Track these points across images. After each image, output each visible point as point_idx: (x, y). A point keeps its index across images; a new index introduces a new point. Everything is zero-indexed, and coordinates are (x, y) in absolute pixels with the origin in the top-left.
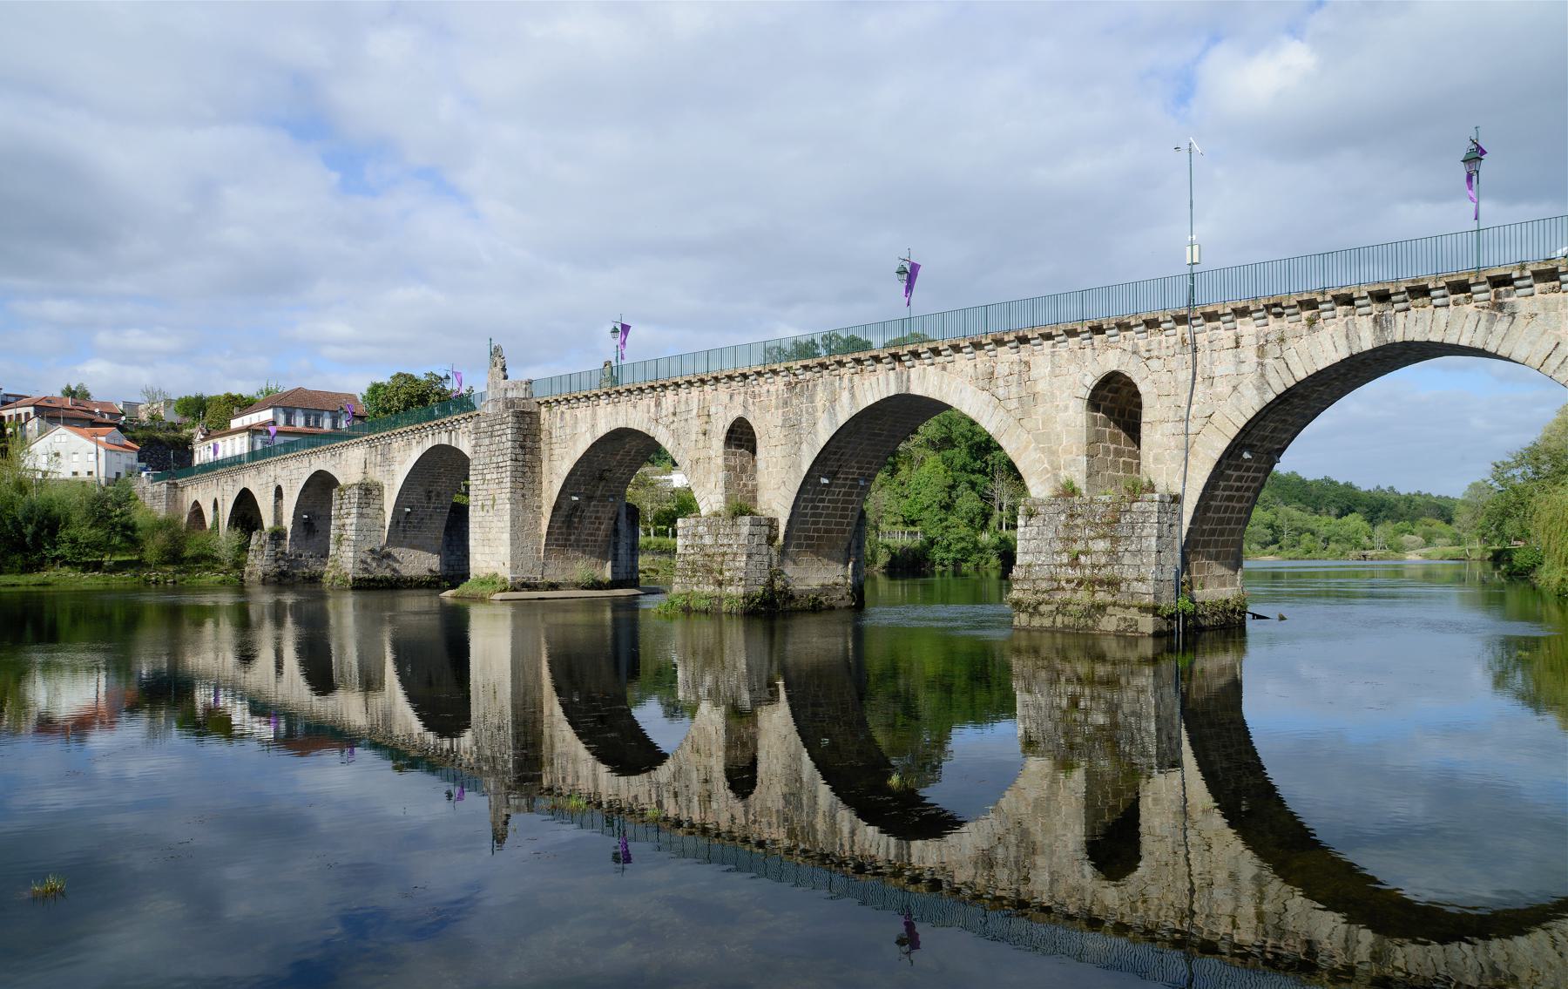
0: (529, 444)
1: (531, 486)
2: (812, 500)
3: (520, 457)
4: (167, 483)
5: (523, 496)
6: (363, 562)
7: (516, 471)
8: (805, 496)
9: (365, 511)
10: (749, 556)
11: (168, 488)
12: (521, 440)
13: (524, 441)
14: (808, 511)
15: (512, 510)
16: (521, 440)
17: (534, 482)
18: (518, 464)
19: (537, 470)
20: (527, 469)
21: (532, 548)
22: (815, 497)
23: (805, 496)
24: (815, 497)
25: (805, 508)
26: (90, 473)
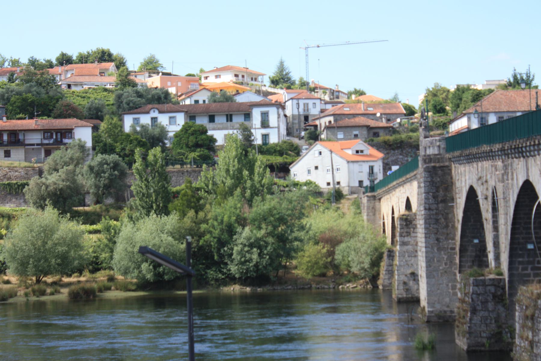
0: (441, 193)
1: (445, 231)
2: (529, 263)
3: (434, 207)
4: (367, 196)
5: (438, 239)
6: (405, 283)
7: (430, 218)
8: (520, 259)
9: (406, 239)
10: (474, 311)
11: (368, 200)
12: (434, 191)
13: (437, 191)
14: (529, 271)
15: (426, 252)
16: (434, 191)
17: (447, 226)
18: (432, 212)
19: (450, 216)
20: (440, 216)
21: (447, 285)
22: (531, 259)
23: (520, 259)
24: (531, 259)
25: (526, 269)
26: (329, 184)
